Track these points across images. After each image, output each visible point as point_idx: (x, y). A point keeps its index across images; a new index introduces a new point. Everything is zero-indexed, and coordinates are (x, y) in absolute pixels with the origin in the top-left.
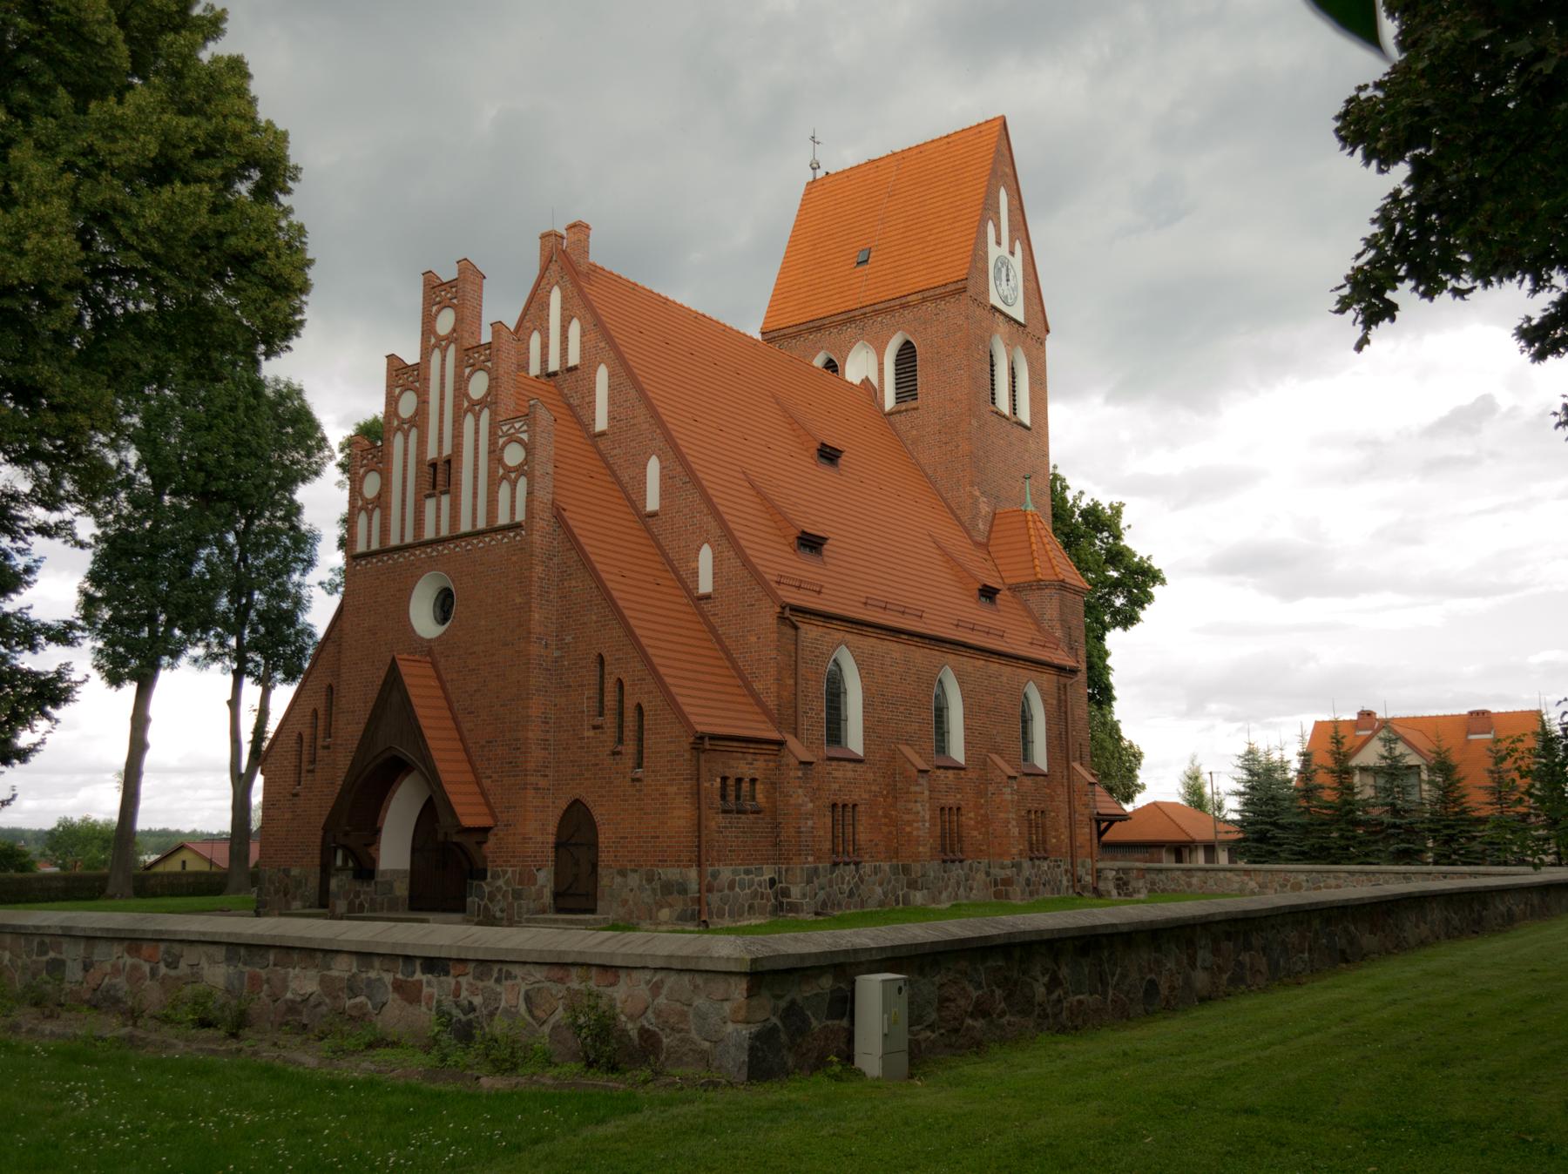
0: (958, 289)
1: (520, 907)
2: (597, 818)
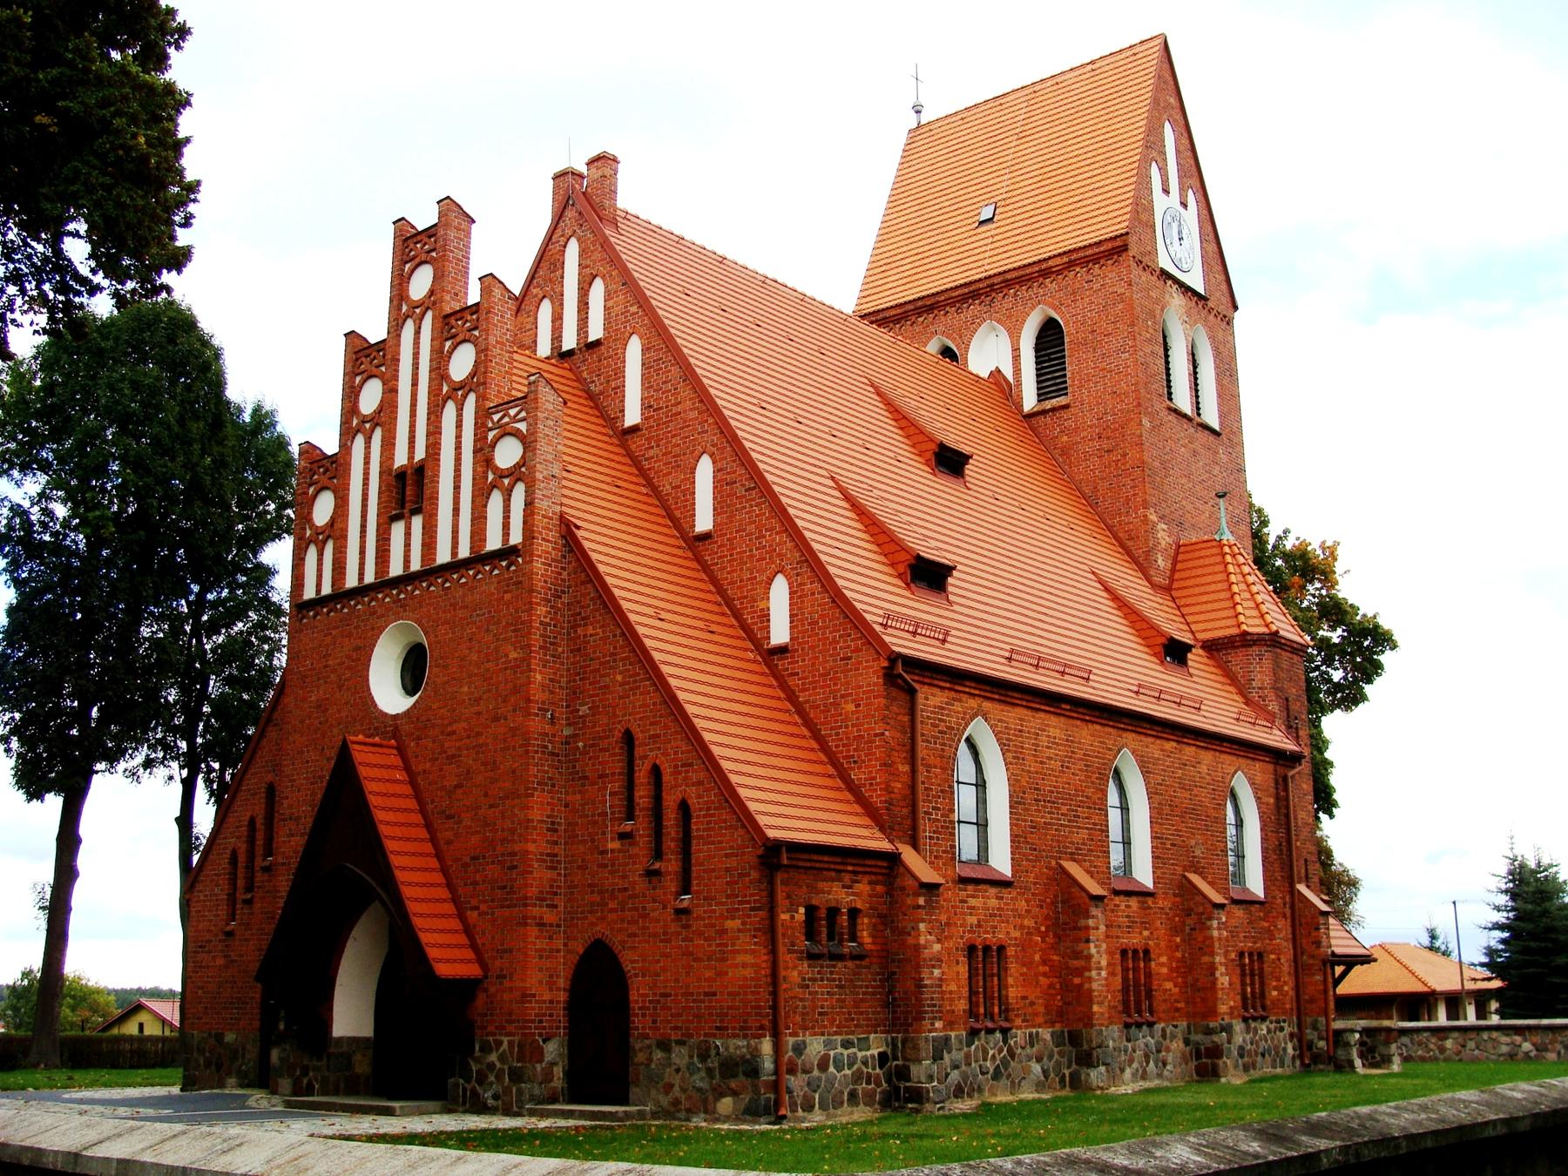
0: (1114, 250)
1: (520, 1092)
2: (628, 967)
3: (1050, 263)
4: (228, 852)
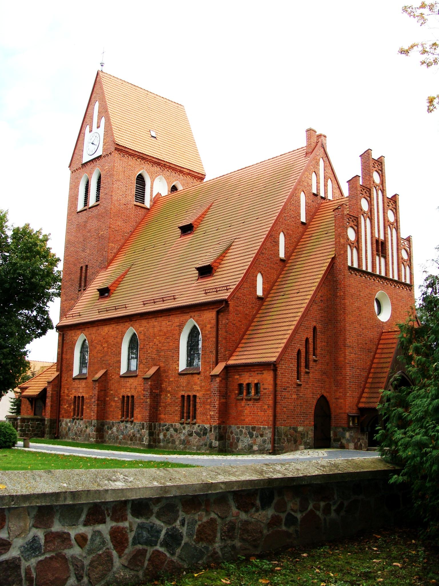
3: (184, 170)
4: (296, 351)
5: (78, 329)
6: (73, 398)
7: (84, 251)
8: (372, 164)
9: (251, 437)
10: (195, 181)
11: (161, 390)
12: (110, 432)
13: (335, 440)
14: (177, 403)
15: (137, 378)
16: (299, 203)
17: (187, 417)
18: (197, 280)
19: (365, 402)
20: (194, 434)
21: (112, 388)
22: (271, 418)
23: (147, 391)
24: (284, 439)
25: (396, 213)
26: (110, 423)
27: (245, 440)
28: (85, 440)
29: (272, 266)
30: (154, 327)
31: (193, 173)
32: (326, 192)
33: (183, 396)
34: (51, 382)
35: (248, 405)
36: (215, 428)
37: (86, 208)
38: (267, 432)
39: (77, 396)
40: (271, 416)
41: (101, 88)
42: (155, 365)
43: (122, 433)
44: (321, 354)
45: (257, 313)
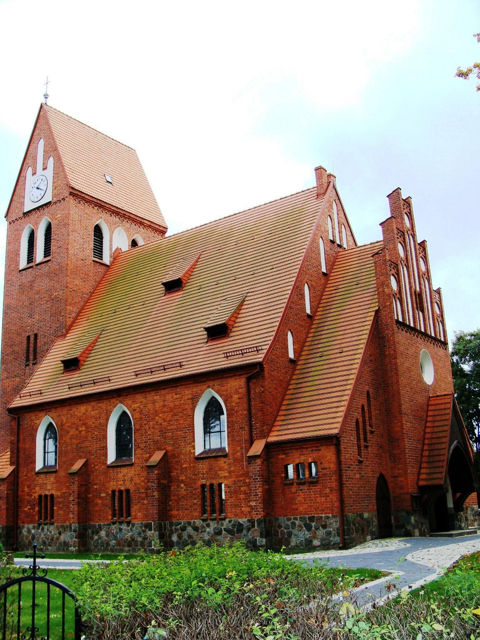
3: (145, 221)
5: (40, 411)
6: (37, 497)
7: (31, 316)
8: (400, 205)
9: (309, 528)
10: (156, 235)
11: (170, 480)
12: (96, 537)
13: (397, 527)
14: (196, 494)
15: (133, 467)
16: (319, 250)
17: (211, 511)
18: (207, 342)
19: (426, 480)
20: (224, 532)
21: (97, 481)
22: (337, 504)
23: (153, 482)
24: (353, 529)
25: (427, 262)
26: (95, 526)
27: (301, 534)
28: (58, 549)
29: (301, 323)
30: (154, 402)
31: (154, 225)
32: (341, 240)
33: (203, 486)
34: (6, 479)
35: (302, 490)
36: (259, 522)
37: (30, 265)
38: (332, 521)
39: (43, 494)
40: (335, 501)
41: (48, 123)
42: (159, 449)
43: (115, 538)
44: (376, 424)
45: (291, 379)
